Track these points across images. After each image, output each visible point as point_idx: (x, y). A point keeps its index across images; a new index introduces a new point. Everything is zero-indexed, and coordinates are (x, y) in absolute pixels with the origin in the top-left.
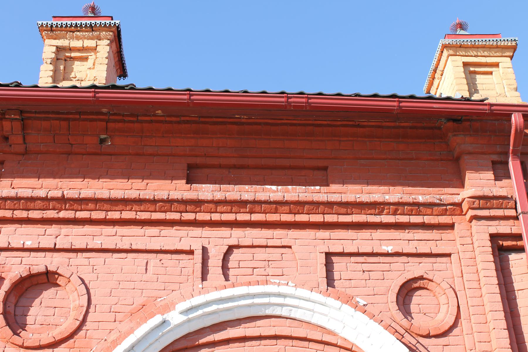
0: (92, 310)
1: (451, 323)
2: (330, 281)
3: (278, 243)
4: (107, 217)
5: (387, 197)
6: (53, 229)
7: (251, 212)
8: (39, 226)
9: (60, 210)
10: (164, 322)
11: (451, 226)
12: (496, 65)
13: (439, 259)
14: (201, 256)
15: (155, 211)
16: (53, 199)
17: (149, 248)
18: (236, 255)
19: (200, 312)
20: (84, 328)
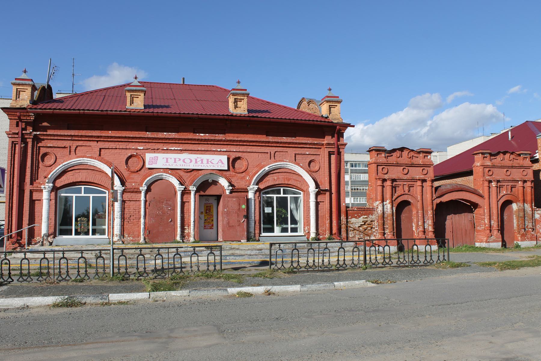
7: (280, 144)
10: (265, 170)
11: (321, 148)
12: (337, 106)
19: (271, 167)
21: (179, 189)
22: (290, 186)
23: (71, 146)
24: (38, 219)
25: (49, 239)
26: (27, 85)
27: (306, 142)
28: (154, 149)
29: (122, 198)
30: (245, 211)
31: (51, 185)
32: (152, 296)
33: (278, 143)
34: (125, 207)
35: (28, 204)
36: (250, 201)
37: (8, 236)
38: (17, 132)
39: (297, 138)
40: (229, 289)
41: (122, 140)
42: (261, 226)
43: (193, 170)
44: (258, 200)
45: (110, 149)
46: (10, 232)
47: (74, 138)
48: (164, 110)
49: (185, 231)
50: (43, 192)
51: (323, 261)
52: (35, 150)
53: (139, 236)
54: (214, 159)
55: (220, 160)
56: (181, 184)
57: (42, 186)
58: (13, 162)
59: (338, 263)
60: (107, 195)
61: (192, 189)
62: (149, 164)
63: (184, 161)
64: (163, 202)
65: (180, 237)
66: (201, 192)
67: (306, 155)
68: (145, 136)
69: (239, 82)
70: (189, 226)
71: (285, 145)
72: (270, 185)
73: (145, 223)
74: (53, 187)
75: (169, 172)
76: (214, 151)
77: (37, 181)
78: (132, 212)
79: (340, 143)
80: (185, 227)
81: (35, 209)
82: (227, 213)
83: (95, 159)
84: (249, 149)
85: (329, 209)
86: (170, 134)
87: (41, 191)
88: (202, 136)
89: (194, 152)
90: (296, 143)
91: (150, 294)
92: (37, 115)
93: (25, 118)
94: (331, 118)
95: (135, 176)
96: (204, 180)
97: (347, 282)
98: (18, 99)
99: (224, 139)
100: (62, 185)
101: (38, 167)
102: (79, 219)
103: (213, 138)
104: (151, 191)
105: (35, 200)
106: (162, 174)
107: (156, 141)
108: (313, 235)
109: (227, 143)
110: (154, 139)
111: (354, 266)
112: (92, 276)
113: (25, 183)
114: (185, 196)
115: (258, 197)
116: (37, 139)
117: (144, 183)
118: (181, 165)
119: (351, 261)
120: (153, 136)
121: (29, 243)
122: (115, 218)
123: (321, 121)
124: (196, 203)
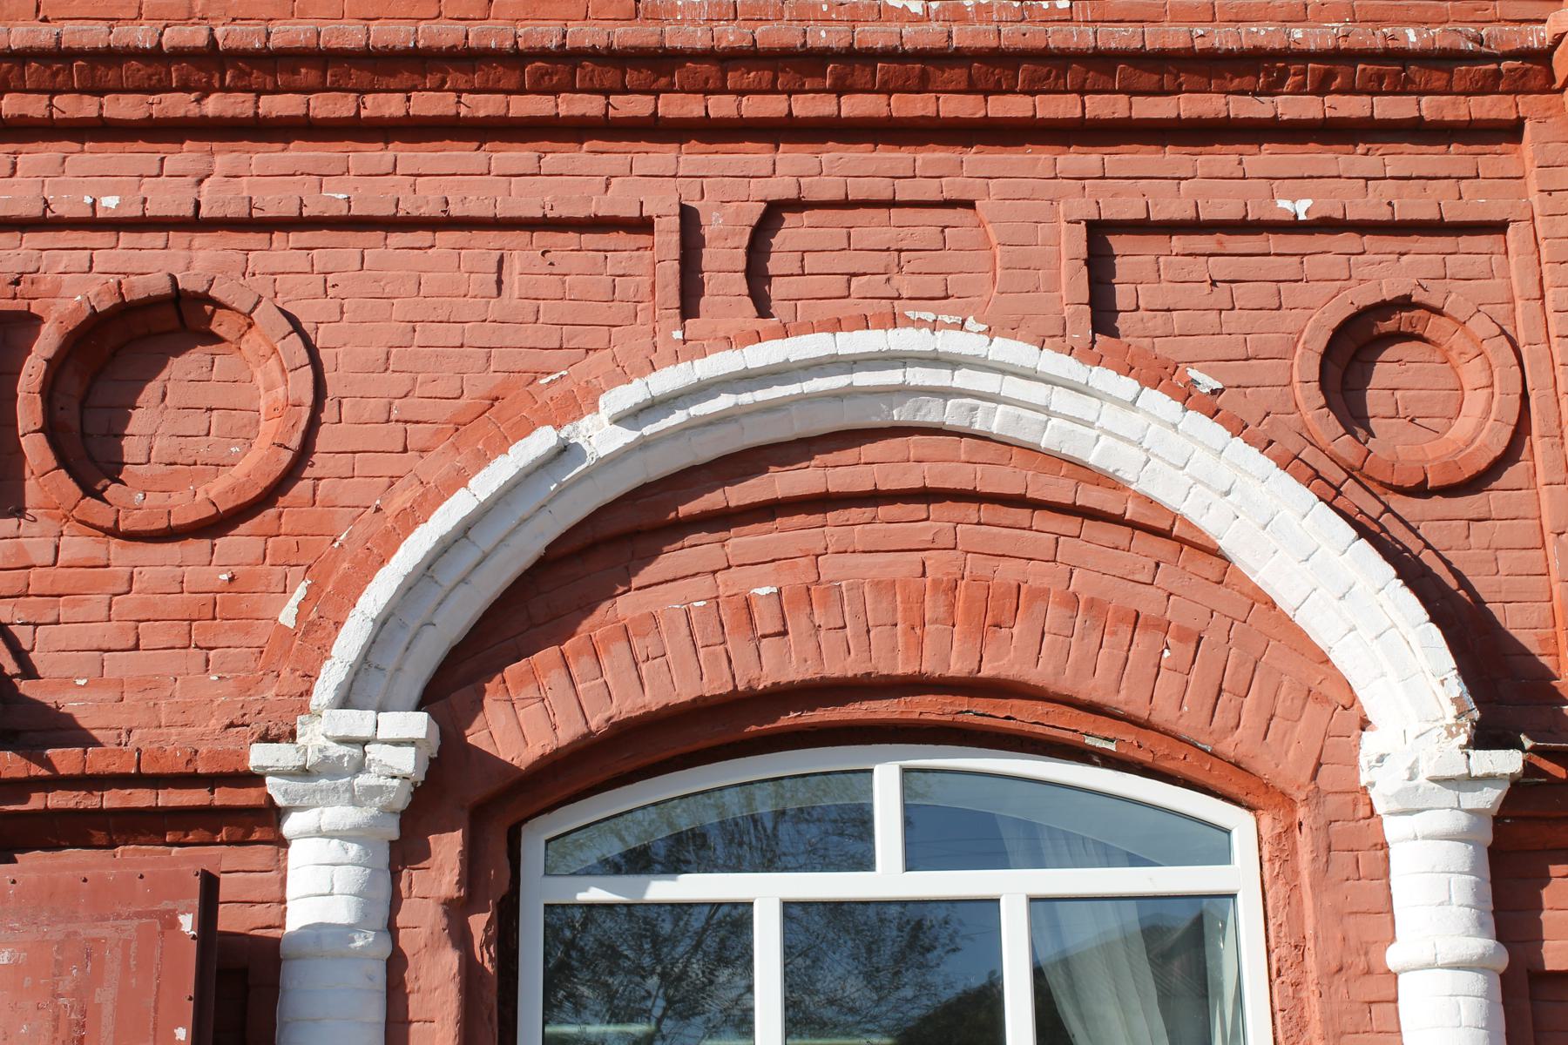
0: (328, 414)
1: (1498, 450)
2: (1103, 315)
3: (930, 191)
4: (364, 113)
5: (1298, 34)
6: (186, 156)
7: (840, 90)
8: (141, 145)
9: (206, 92)
10: (564, 451)
11: (1511, 131)
13: (1465, 242)
14: (676, 238)
15: (521, 91)
18: (792, 234)
19: (678, 417)
20: (308, 472)
22: (1023, 715)
44: (450, 959)
67: (1274, 242)
115: (456, 911)
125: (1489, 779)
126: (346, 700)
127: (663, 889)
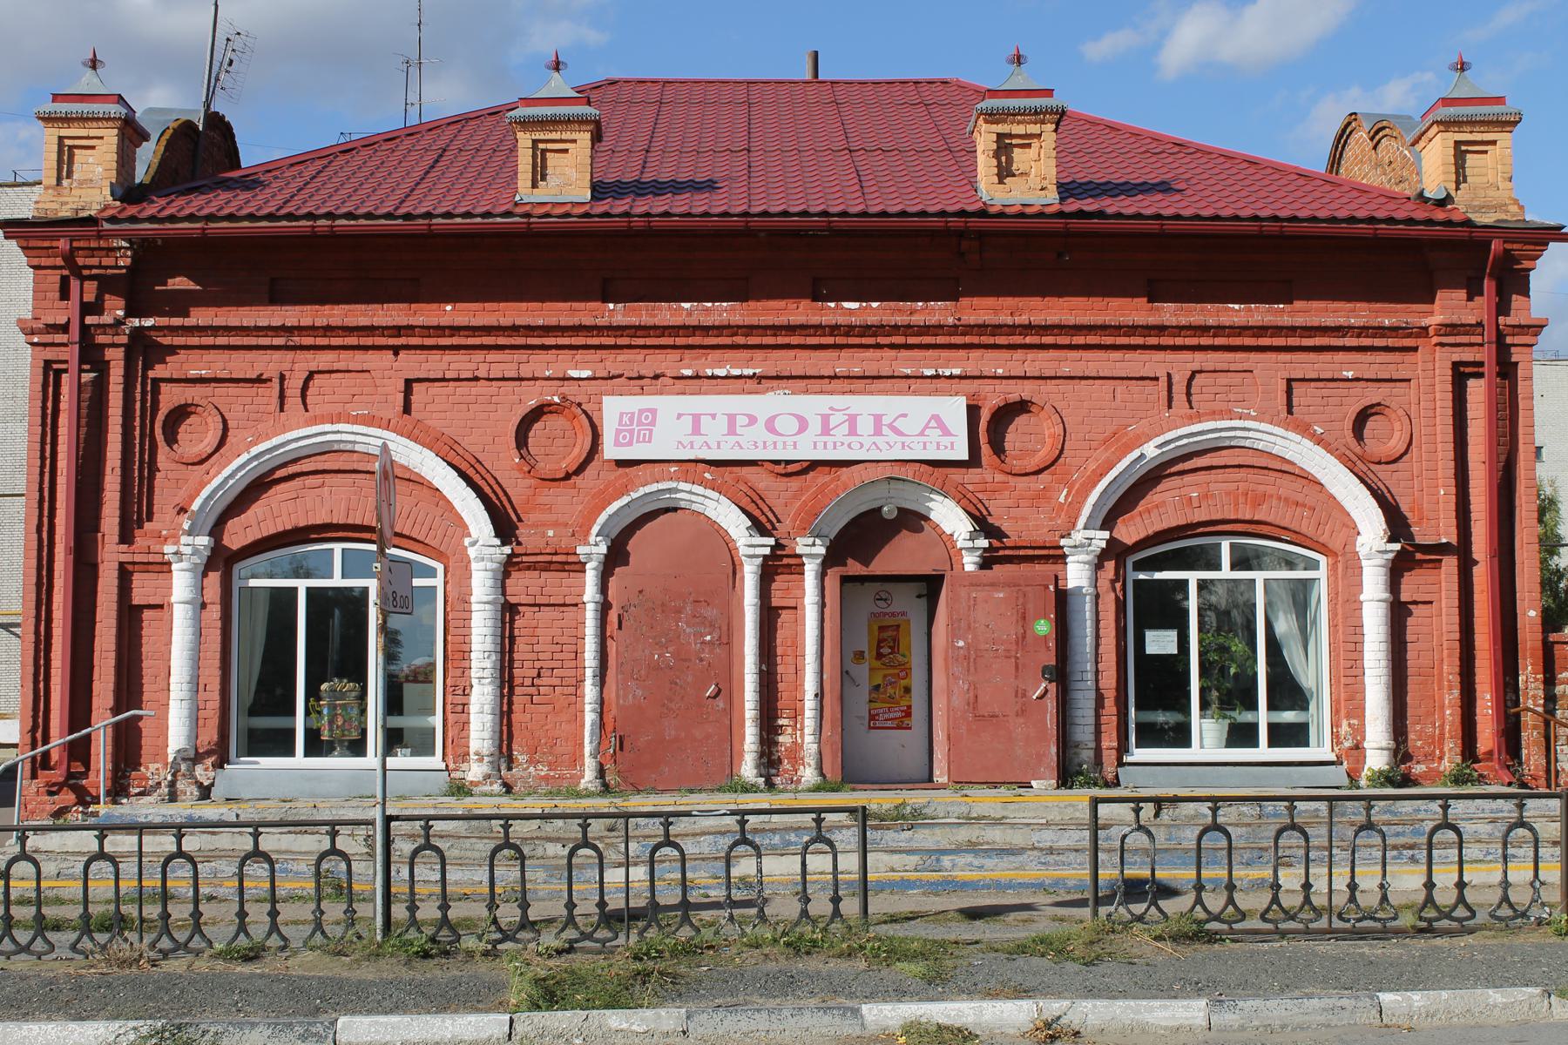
1: (1402, 451)
5: (1353, 321)
7: (1215, 336)
10: (1142, 456)
11: (1415, 349)
12: (1494, 143)
13: (1398, 384)
16: (1020, 326)
17: (1115, 375)
18: (1198, 379)
19: (1172, 446)
21: (751, 551)
23: (287, 374)
24: (155, 687)
25: (199, 770)
26: (98, 119)
27: (1342, 321)
28: (640, 378)
29: (504, 594)
30: (1048, 648)
31: (204, 541)
32: (519, 1028)
33: (1203, 330)
34: (516, 632)
35: (113, 622)
36: (1073, 603)
37: (34, 758)
38: (62, 320)
39: (1298, 304)
40: (869, 1006)
41: (502, 341)
42: (1126, 714)
43: (814, 465)
44: (1113, 595)
45: (451, 384)
46: (40, 743)
47: (296, 340)
48: (699, 203)
49: (781, 739)
50: (171, 571)
51: (1353, 886)
52: (138, 396)
53: (576, 759)
54: (904, 416)
55: (936, 418)
56: (760, 527)
57: (169, 549)
58: (48, 448)
59: (1429, 900)
60: (438, 582)
61: (807, 550)
62: (617, 444)
63: (770, 426)
64: (679, 611)
65: (758, 767)
66: (850, 561)
67: (1341, 384)
68: (600, 322)
69: (1018, 59)
70: (797, 714)
71: (1237, 341)
72: (1165, 525)
73: (602, 702)
74: (213, 550)
75: (707, 475)
76: (907, 377)
77: (147, 525)
78: (548, 656)
79: (1510, 320)
80: (780, 722)
81: (141, 645)
82: (966, 658)
83: (387, 429)
84: (1070, 363)
85: (1457, 636)
86: (707, 309)
87: (165, 567)
88: (851, 312)
89: (815, 385)
90: (1292, 330)
91: (512, 1021)
92: (145, 249)
93: (94, 261)
94: (1465, 204)
95: (559, 496)
96: (864, 508)
97: (1445, 994)
98: (65, 182)
99: (951, 321)
100: (250, 540)
101: (153, 469)
102: (324, 686)
103: (899, 319)
104: (627, 564)
105: (142, 608)
106: (673, 485)
107: (649, 341)
108: (1377, 759)
109: (968, 339)
110: (639, 333)
111: (1511, 915)
112: (296, 934)
113: (100, 535)
114: (779, 583)
115: (1113, 582)
116: (144, 350)
117: (595, 529)
118: (761, 445)
119: (1499, 892)
120: (634, 320)
121: (118, 791)
122: (474, 682)
123: (1410, 221)
124: (827, 610)
125: (1391, 551)
126: (1085, 528)
127: (1158, 575)
